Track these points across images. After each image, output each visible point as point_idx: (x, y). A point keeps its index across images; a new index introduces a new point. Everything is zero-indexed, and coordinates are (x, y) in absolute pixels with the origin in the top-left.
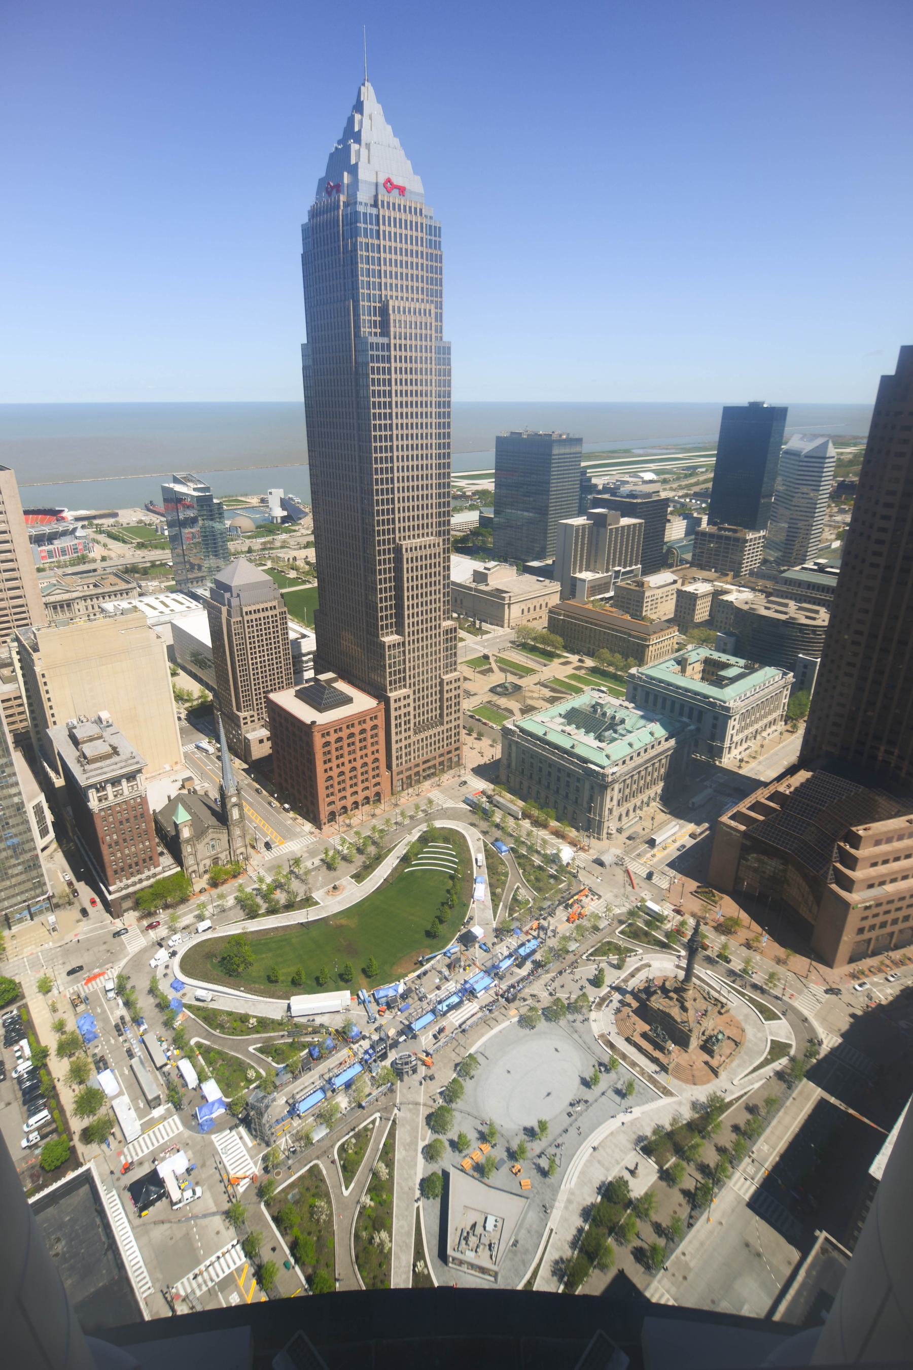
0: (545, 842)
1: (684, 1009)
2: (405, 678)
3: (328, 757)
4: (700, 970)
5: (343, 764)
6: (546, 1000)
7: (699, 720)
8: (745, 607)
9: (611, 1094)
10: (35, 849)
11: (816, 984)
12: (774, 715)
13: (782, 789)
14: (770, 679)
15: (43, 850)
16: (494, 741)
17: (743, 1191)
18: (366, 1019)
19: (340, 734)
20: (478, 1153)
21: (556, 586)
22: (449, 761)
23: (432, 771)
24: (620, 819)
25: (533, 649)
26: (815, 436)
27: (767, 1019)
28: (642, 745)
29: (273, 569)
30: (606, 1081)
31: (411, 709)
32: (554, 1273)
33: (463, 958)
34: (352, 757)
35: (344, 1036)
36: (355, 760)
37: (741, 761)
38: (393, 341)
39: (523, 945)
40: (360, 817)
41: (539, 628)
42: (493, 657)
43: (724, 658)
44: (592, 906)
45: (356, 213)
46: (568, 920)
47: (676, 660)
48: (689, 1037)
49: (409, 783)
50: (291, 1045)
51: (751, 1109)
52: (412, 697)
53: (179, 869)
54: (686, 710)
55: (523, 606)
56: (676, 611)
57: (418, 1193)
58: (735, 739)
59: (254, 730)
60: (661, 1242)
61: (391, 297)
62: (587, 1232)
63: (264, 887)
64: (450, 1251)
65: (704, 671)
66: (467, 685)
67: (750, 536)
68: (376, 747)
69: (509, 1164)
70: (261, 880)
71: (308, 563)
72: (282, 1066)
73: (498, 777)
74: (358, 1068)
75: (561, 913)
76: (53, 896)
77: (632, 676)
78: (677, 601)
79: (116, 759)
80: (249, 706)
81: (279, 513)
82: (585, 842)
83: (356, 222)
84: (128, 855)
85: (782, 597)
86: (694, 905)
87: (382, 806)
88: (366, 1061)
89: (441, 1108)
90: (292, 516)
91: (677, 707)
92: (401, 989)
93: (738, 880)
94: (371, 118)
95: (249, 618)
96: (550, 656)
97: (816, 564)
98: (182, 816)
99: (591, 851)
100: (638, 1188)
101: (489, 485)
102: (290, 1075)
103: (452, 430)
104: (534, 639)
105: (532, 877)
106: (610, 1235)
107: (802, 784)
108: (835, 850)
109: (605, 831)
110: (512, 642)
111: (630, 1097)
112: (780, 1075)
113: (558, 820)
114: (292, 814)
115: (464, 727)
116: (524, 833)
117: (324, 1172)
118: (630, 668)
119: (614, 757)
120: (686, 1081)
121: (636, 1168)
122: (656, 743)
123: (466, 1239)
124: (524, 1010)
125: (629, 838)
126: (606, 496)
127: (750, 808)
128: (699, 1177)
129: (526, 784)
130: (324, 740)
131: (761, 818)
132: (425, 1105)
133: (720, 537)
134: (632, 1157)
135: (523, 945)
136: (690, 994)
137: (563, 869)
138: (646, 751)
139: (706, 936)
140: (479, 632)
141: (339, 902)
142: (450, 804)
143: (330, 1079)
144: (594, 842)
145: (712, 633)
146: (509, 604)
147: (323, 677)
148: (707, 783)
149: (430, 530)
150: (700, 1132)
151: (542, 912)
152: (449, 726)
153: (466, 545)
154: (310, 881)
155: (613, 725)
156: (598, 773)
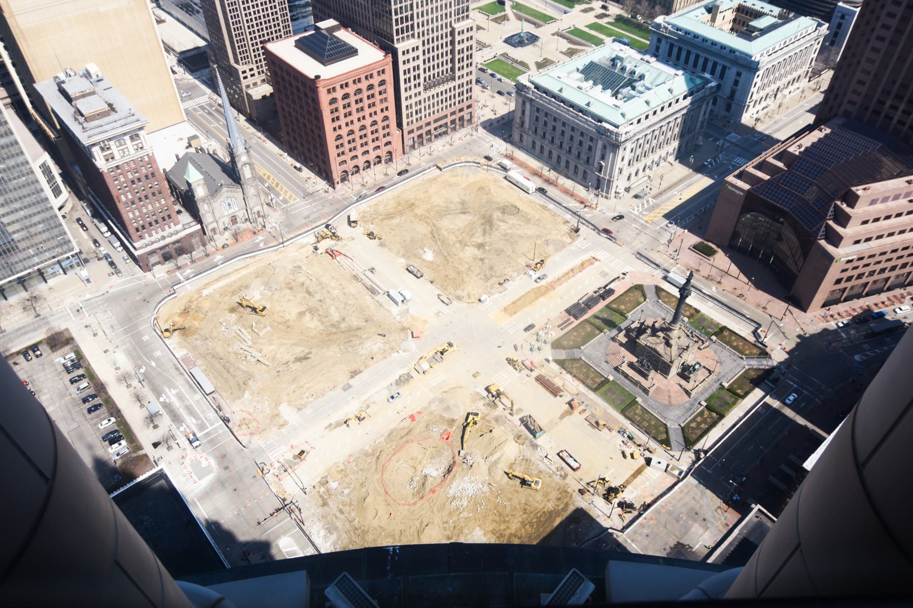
3: (336, 114)
7: (722, 76)
10: (51, 208)
12: (801, 71)
13: (791, 150)
15: (60, 209)
19: (346, 90)
23: (444, 129)
24: (629, 178)
34: (361, 114)
36: (364, 118)
37: (757, 120)
48: (670, 367)
52: (421, 49)
53: (199, 227)
54: (710, 65)
58: (754, 98)
59: (255, 84)
65: (734, 20)
66: (479, 36)
73: (510, 136)
76: (81, 252)
77: (658, 26)
79: (114, 116)
84: (146, 214)
86: (693, 259)
98: (194, 176)
107: (813, 144)
108: (832, 209)
109: (613, 190)
119: (628, 117)
125: (636, 197)
130: (330, 97)
136: (675, 334)
138: (662, 109)
152: (460, 82)
156: (611, 132)
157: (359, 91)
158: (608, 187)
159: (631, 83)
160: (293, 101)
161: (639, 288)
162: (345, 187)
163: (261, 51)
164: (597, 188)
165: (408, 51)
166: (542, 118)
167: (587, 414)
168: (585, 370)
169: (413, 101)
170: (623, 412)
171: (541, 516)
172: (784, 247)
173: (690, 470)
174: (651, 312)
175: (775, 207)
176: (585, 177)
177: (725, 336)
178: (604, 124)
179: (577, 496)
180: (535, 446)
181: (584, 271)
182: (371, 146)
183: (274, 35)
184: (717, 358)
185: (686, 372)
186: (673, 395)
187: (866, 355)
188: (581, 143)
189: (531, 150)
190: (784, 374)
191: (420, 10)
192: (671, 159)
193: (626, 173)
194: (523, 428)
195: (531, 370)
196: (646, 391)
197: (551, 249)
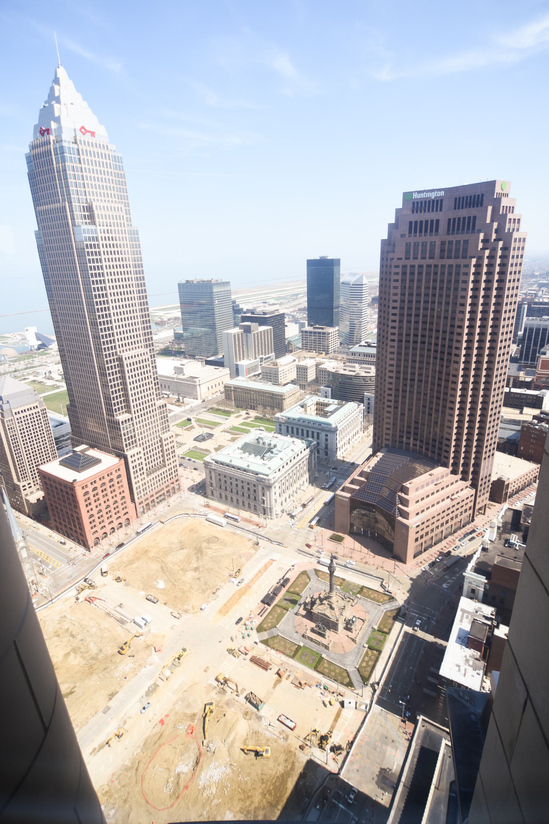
2: (135, 441)
7: (318, 438)
8: (333, 371)
13: (365, 470)
23: (163, 497)
24: (282, 504)
37: (343, 457)
43: (326, 400)
45: (62, 148)
52: (142, 452)
54: (310, 433)
58: (338, 446)
61: (94, 200)
65: (317, 409)
66: (179, 439)
67: (330, 330)
73: (205, 493)
80: (25, 477)
86: (331, 546)
95: (18, 416)
96: (227, 413)
97: (366, 342)
103: (146, 281)
107: (376, 465)
108: (397, 498)
109: (274, 513)
119: (273, 469)
144: (268, 521)
152: (169, 467)
153: (166, 352)
156: (265, 479)
157: (104, 484)
158: (271, 512)
159: (270, 450)
160: (59, 499)
161: (304, 573)
162: (98, 549)
163: (36, 471)
164: (264, 514)
165: (134, 455)
166: (223, 479)
167: (291, 678)
168: (283, 643)
169: (140, 484)
170: (316, 669)
171: (276, 781)
172: (379, 526)
173: (372, 701)
174: (316, 587)
175: (367, 504)
176: (255, 509)
177: (365, 593)
178: (260, 475)
179: (299, 752)
180: (259, 718)
181: (268, 570)
182: (115, 517)
183: (46, 460)
184: (365, 610)
185: (348, 626)
186: (345, 645)
187: (449, 583)
188: (249, 489)
189: (221, 498)
190: (407, 609)
191: (139, 431)
193: (279, 502)
194: (248, 705)
195: (246, 654)
196: (327, 647)
197: (243, 560)
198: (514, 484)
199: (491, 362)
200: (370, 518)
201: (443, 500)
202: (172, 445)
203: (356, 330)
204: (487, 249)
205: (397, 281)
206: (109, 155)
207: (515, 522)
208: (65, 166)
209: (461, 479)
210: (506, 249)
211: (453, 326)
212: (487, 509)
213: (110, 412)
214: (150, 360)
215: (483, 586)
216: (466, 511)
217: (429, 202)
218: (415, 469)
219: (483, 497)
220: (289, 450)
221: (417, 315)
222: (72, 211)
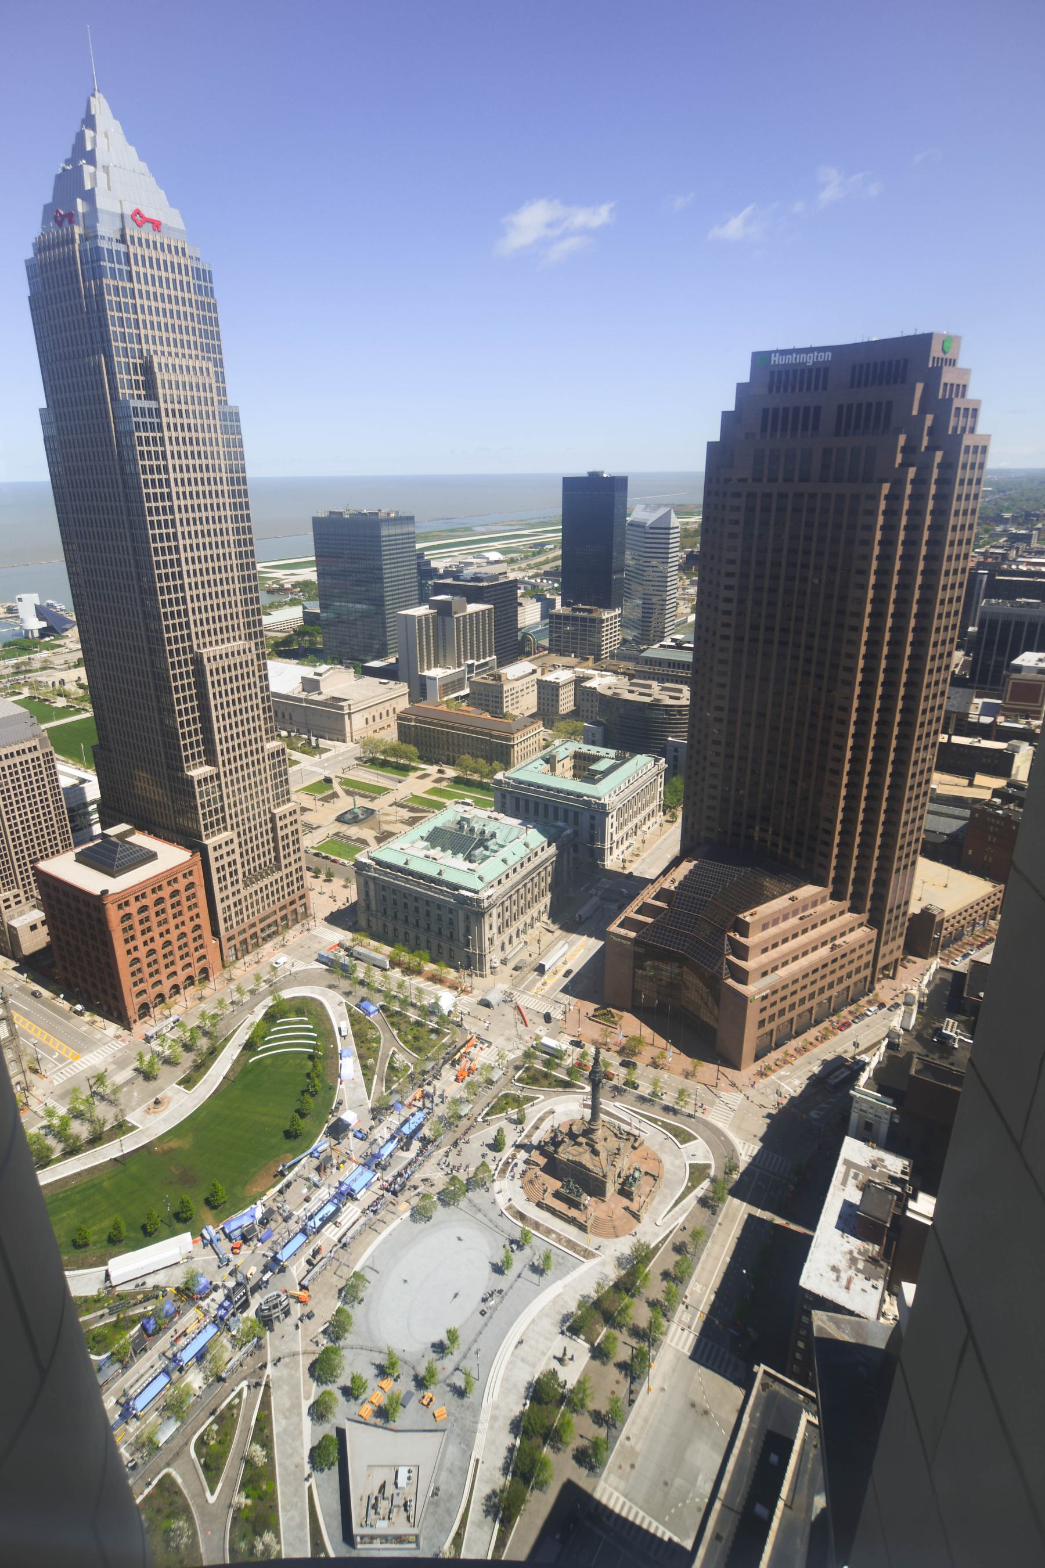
0: (420, 991)
1: (595, 1153)
2: (224, 819)
4: (607, 1104)
5: (152, 940)
6: (440, 1179)
7: (576, 822)
8: (609, 693)
9: (528, 1273)
11: (727, 1091)
13: (666, 886)
14: (643, 768)
16: (347, 880)
17: (681, 1344)
18: (217, 1263)
20: (377, 1393)
21: (403, 688)
22: (295, 914)
23: (273, 929)
24: (503, 949)
25: (384, 764)
26: (659, 506)
27: (683, 1142)
28: (517, 858)
29: (32, 698)
30: (520, 1260)
31: (237, 856)
32: (487, 1512)
33: (334, 1155)
34: (163, 928)
35: (188, 1293)
36: (168, 932)
37: (624, 861)
38: (163, 406)
39: (406, 1121)
40: (183, 1003)
41: (388, 739)
42: (334, 778)
43: (594, 750)
44: (482, 1056)
45: (98, 250)
46: (457, 1080)
47: (543, 758)
48: (604, 1184)
49: (245, 948)
50: (115, 1325)
51: (679, 1249)
52: (236, 841)
54: (561, 813)
55: (367, 714)
56: (539, 703)
57: (307, 1469)
58: (615, 838)
59: (22, 913)
60: (602, 1432)
61: (156, 352)
62: (520, 1449)
63: (56, 1122)
64: (356, 1530)
65: (574, 767)
66: (308, 818)
67: (606, 615)
68: (195, 911)
69: (417, 1395)
70: (50, 1113)
71: (81, 686)
72: (104, 1356)
73: (356, 923)
74: (211, 1330)
75: (448, 1073)
77: (499, 782)
78: (539, 693)
81: (35, 624)
82: (467, 982)
83: (99, 260)
85: (645, 678)
87: (212, 985)
88: (222, 1318)
89: (326, 1351)
90: (53, 629)
91: (551, 810)
92: (259, 1211)
93: (636, 993)
94: (107, 136)
96: (405, 769)
97: (673, 640)
99: (475, 992)
100: (570, 1376)
101: (310, 574)
102: (118, 1366)
103: (251, 512)
104: (384, 752)
105: (410, 1037)
106: (544, 1443)
107: (685, 877)
108: (726, 942)
109: (488, 966)
110: (359, 759)
111: (549, 1272)
112: (703, 1202)
113: (433, 961)
114: (87, 1017)
115: (308, 869)
116: (394, 986)
117: (179, 1481)
118: (495, 772)
119: (487, 879)
120: (606, 1236)
121: (565, 1354)
122: (532, 855)
123: (375, 1507)
124: (415, 1201)
125: (516, 969)
126: (449, 581)
127: (638, 912)
128: (633, 1342)
129: (390, 926)
130: (122, 913)
131: (650, 920)
132: (305, 1353)
133: (575, 619)
134: (559, 1343)
135: (406, 1121)
136: (599, 1135)
137: (444, 1020)
138: (522, 865)
139: (607, 1065)
140: (317, 750)
141: (165, 1120)
142: (300, 966)
143: (175, 1355)
144: (477, 981)
145: (579, 724)
146: (349, 714)
147: (112, 831)
148: (593, 891)
149: (237, 633)
150: (627, 1291)
151: (420, 1078)
154: (122, 1101)
155: (482, 842)
156: (471, 899)
159: (482, 843)
163: (31, 872)
165: (220, 846)
183: (49, 851)
192: (545, 917)
198: (952, 921)
199: (914, 685)
200: (671, 981)
201: (815, 949)
202: (293, 828)
203: (656, 616)
204: (912, 465)
205: (737, 522)
206: (186, 266)
207: (951, 996)
208: (101, 283)
209: (851, 910)
210: (948, 466)
211: (841, 612)
212: (900, 968)
213: (174, 764)
214: (256, 663)
215: (888, 1117)
216: (858, 970)
217: (803, 371)
218: (762, 886)
219: (891, 945)
220: (519, 843)
221: (773, 590)
222: (111, 374)
